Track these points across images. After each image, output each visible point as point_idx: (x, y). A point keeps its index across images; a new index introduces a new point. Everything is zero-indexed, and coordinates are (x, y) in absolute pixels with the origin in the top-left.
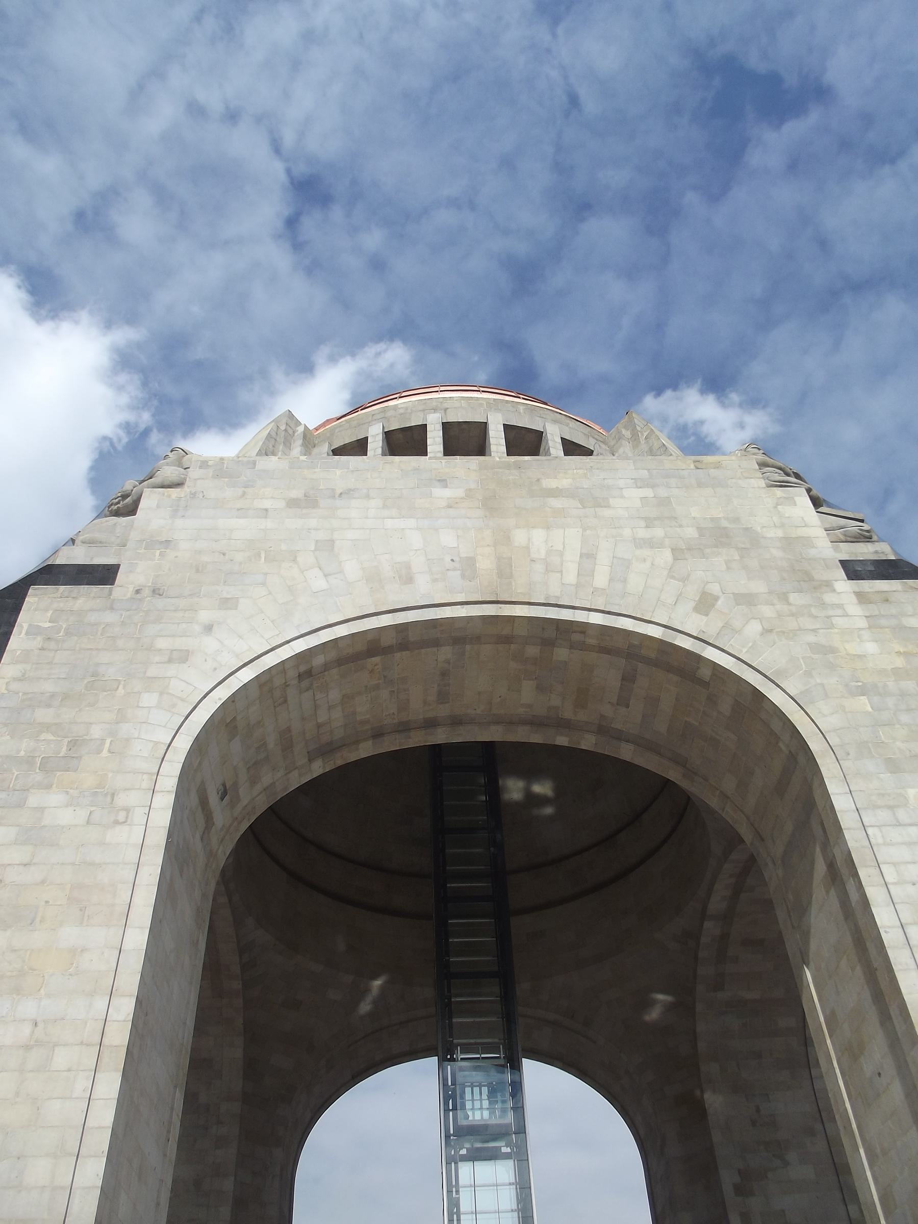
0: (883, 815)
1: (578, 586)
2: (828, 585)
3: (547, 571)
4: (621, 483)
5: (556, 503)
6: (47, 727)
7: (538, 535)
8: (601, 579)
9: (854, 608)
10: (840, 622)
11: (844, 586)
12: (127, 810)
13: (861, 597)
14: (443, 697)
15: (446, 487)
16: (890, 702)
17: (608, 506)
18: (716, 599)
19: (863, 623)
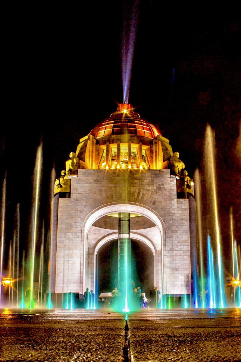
0: (169, 239)
1: (136, 199)
2: (173, 199)
3: (132, 196)
4: (146, 176)
5: (136, 181)
6: (67, 223)
7: (132, 187)
8: (140, 198)
9: (176, 205)
10: (173, 207)
11: (176, 200)
12: (79, 235)
13: (178, 203)
14: (117, 209)
15: (118, 177)
16: (175, 222)
17: (144, 182)
18: (156, 202)
19: (176, 207)
